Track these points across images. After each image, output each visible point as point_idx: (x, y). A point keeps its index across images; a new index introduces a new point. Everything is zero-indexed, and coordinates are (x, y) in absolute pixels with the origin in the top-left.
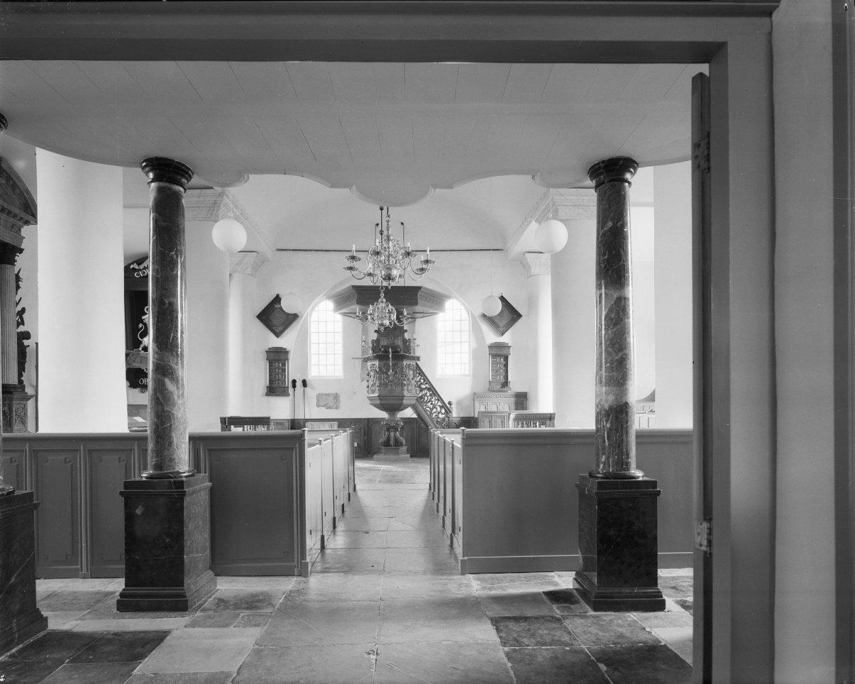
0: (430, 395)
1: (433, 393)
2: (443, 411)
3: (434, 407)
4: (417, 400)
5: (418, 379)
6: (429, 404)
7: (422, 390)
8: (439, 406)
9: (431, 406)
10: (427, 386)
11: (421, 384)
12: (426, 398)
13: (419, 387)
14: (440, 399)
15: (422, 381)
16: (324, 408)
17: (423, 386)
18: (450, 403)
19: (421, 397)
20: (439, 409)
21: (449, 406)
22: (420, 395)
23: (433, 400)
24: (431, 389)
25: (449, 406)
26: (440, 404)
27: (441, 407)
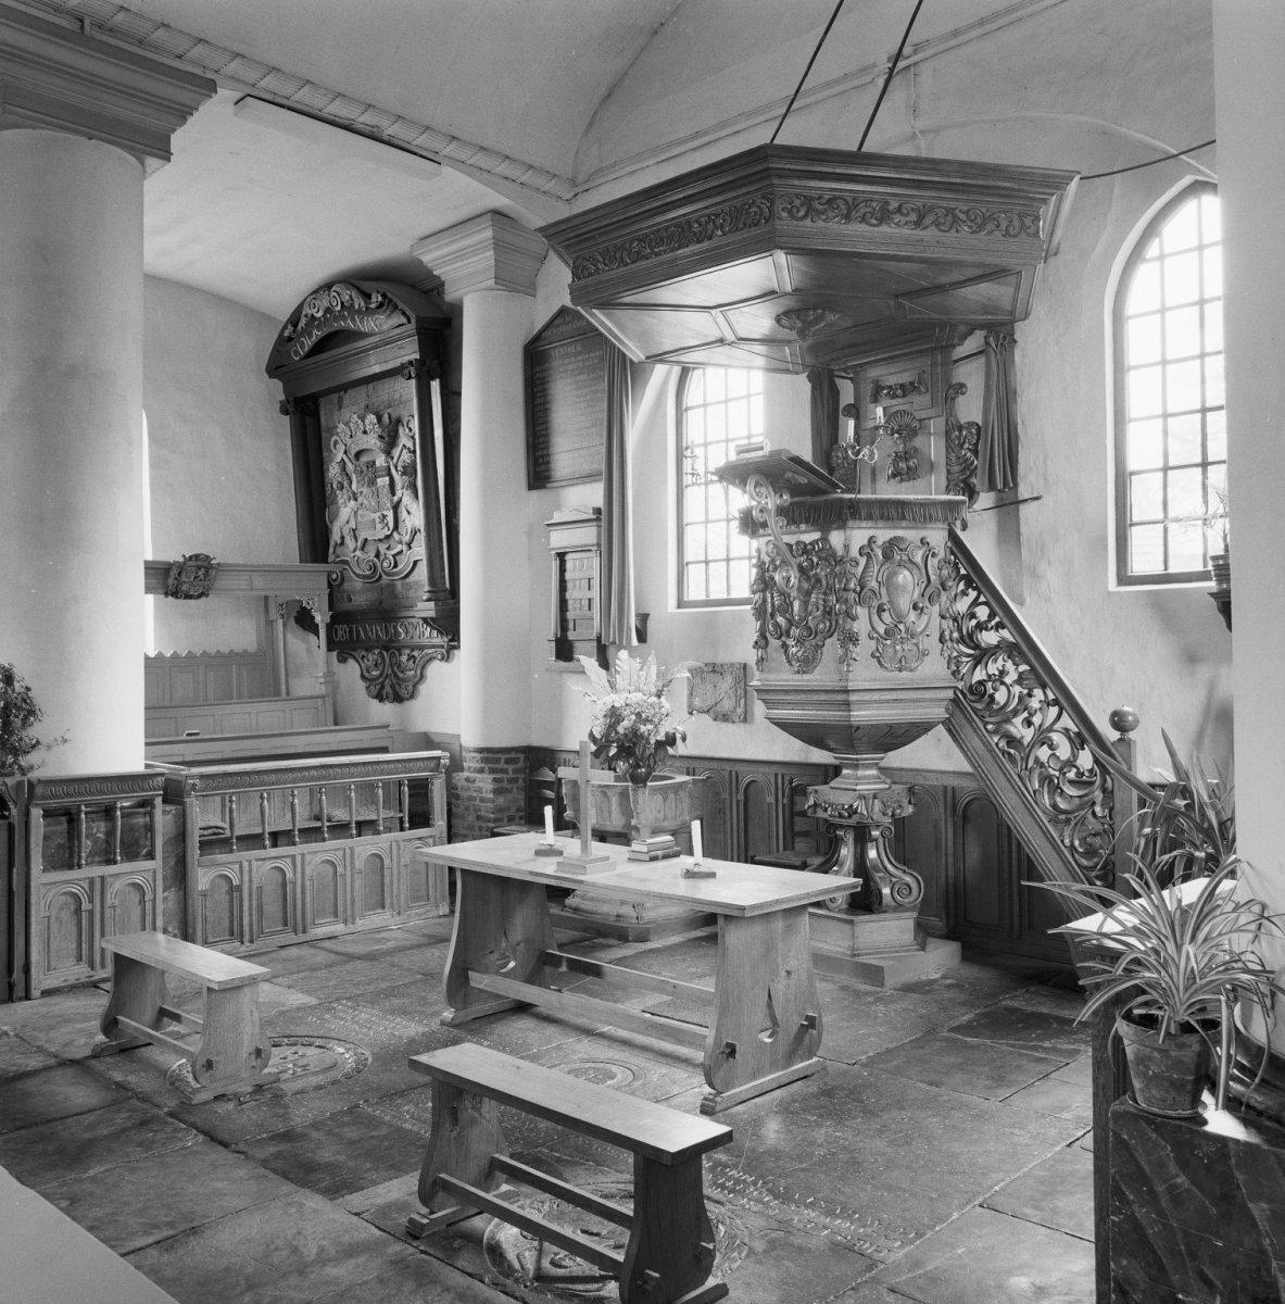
0: (1020, 681)
1: (1033, 669)
2: (1085, 760)
3: (1042, 738)
4: (955, 701)
5: (962, 606)
6: (1018, 721)
7: (982, 655)
8: (1066, 731)
9: (1028, 735)
10: (1005, 633)
11: (981, 627)
12: (1001, 697)
13: (969, 639)
14: (1066, 701)
15: (982, 613)
16: (707, 718)
17: (989, 638)
18: (1119, 721)
19: (978, 691)
20: (1064, 751)
21: (1112, 735)
22: (979, 675)
23: (1035, 703)
24: (1023, 648)
25: (1112, 735)
26: (1067, 721)
27: (1078, 742)
